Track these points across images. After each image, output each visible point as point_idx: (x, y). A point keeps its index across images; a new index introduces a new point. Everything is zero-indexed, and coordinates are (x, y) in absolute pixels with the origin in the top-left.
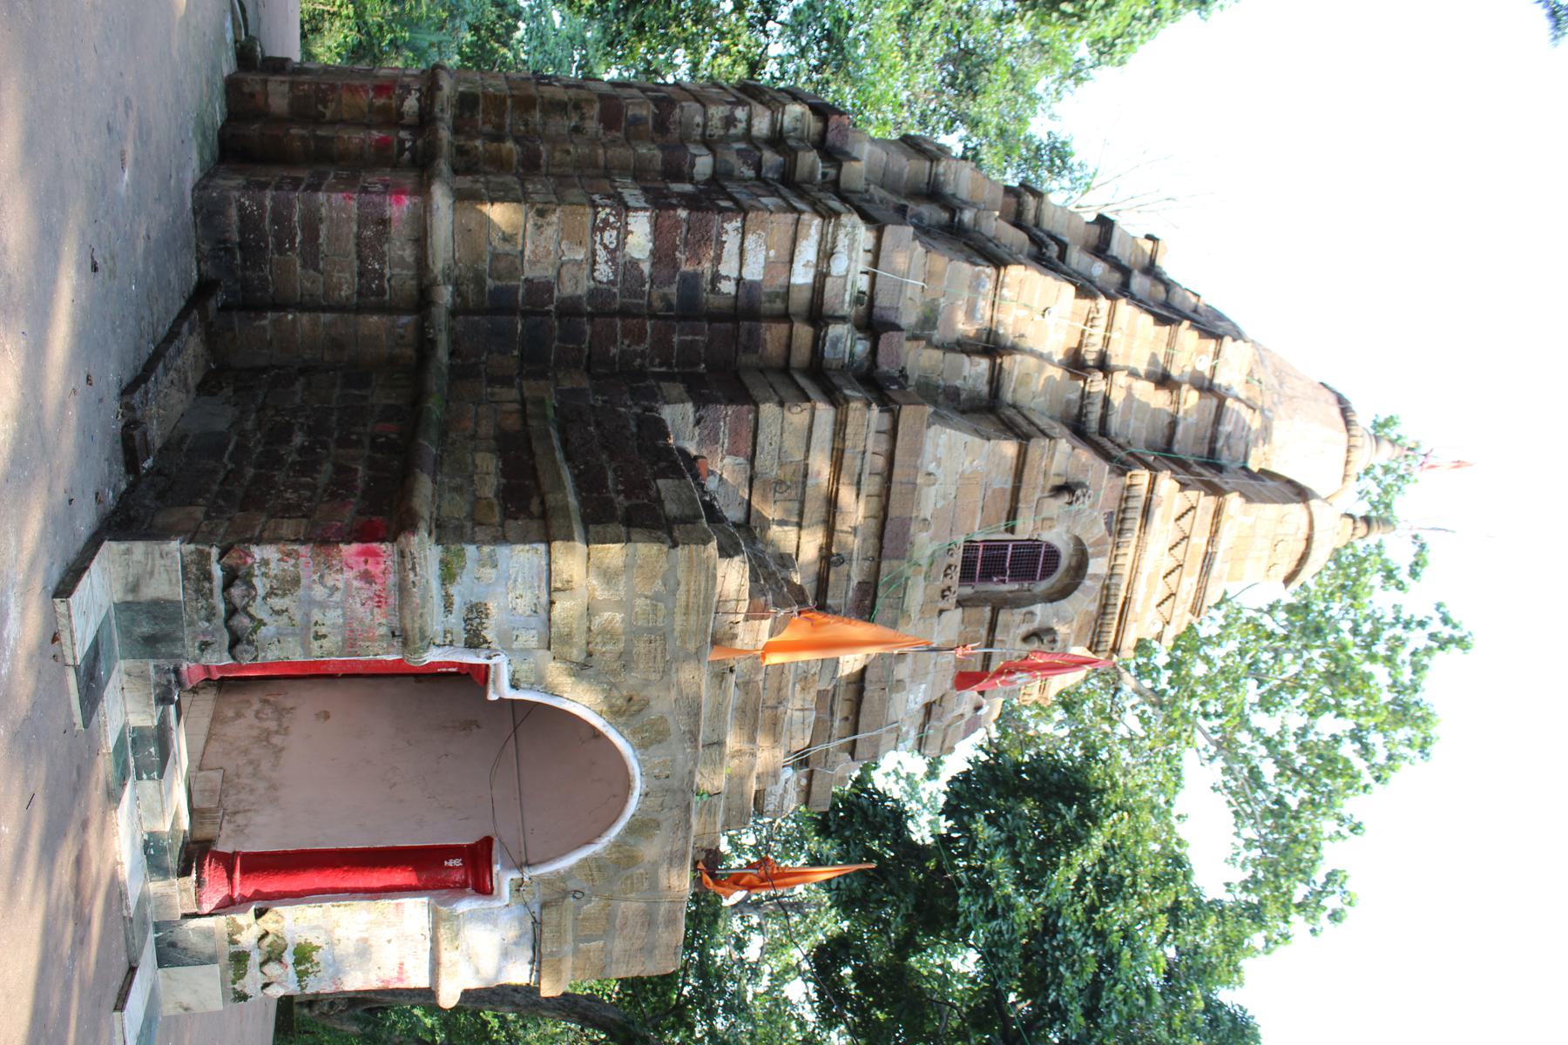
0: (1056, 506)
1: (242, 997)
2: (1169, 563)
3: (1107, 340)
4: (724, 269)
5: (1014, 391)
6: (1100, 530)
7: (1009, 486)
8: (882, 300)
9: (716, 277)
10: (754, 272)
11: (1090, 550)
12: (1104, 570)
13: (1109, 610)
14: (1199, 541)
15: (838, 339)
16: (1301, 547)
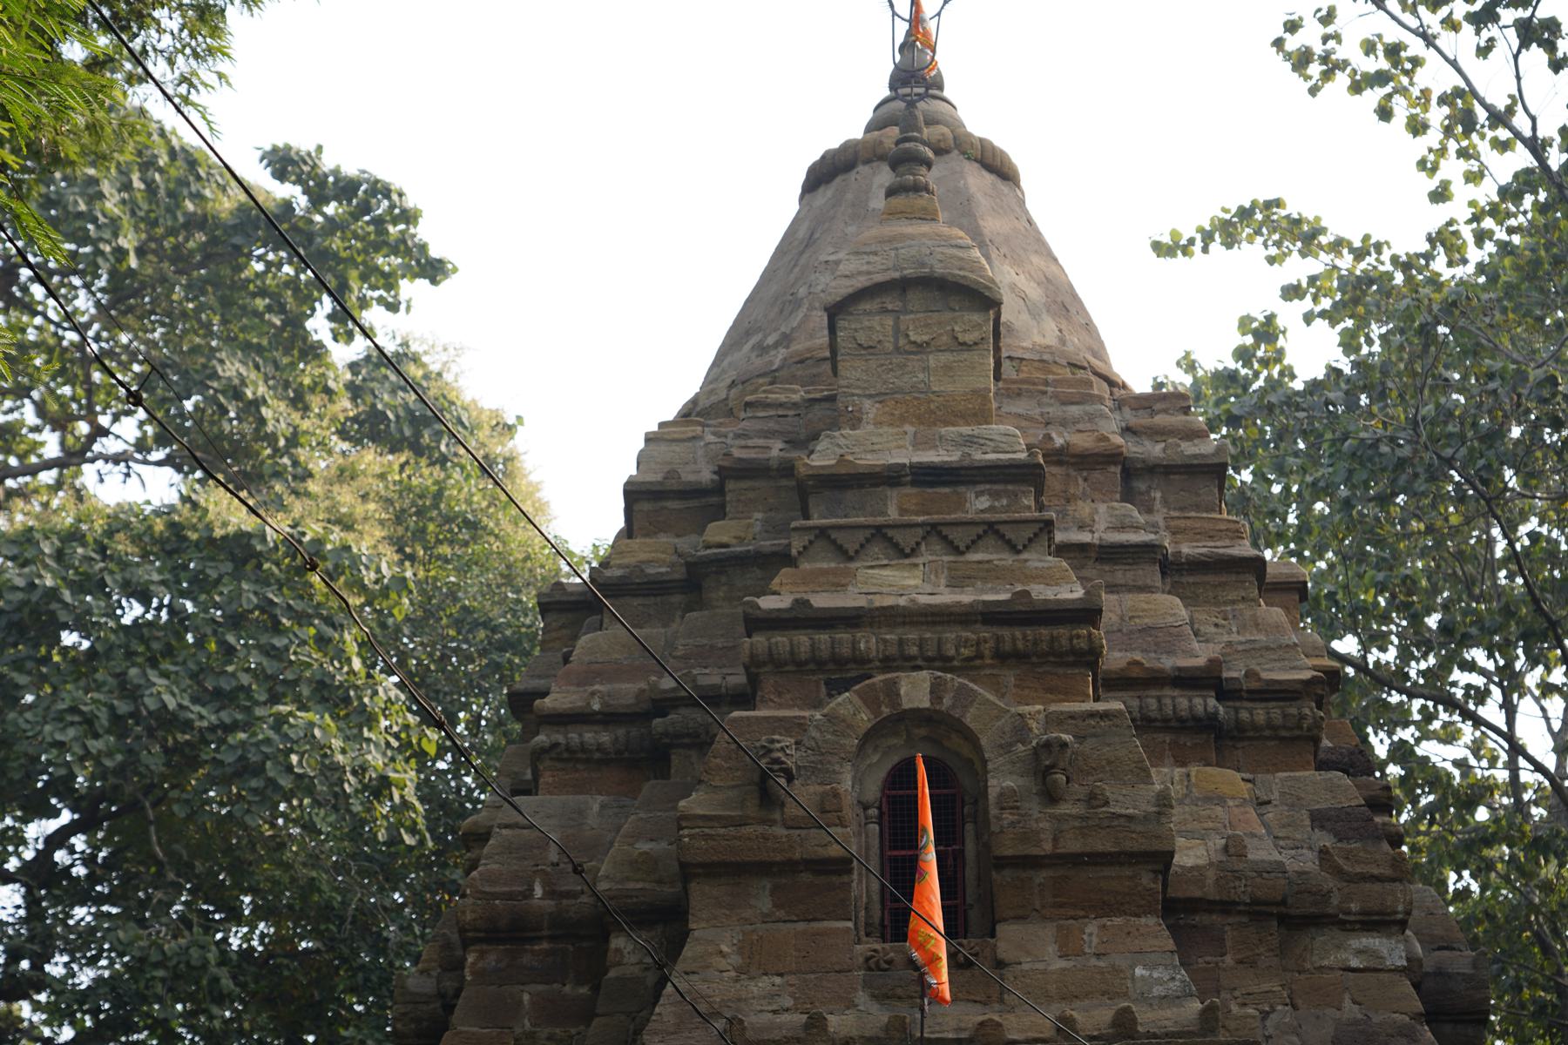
2: (932, 555)
3: (608, 718)
5: (660, 882)
6: (845, 702)
7: (768, 884)
11: (886, 711)
12: (924, 677)
13: (1008, 647)
14: (894, 507)
16: (915, 298)
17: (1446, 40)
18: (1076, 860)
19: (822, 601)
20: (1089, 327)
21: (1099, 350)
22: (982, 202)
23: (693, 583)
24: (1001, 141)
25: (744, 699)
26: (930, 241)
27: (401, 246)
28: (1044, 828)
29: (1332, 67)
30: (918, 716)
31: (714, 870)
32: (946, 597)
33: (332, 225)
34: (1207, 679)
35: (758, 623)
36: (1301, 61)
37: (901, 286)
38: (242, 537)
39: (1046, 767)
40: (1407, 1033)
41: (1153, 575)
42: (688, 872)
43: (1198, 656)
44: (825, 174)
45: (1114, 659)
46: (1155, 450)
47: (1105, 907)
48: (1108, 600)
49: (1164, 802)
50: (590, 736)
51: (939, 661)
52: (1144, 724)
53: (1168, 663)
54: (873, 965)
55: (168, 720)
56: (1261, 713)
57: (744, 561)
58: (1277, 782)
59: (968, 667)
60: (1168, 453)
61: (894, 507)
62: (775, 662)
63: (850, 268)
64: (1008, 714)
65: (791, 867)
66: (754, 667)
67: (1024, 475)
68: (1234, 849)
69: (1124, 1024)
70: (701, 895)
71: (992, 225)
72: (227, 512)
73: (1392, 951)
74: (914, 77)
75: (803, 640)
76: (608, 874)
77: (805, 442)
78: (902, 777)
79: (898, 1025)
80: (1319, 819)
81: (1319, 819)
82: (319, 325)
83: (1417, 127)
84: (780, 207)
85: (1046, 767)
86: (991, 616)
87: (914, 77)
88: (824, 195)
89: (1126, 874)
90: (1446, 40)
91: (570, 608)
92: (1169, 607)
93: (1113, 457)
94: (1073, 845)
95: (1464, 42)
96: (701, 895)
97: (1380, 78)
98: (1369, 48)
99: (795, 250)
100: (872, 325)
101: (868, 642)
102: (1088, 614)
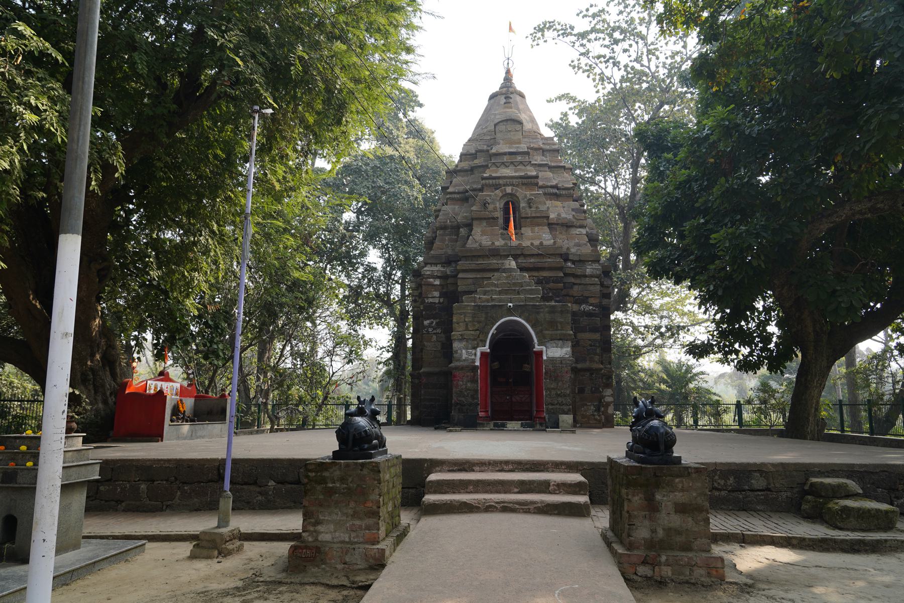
0: (490, 207)
1: (569, 410)
2: (512, 167)
3: (459, 193)
4: (437, 301)
8: (443, 260)
9: (439, 303)
10: (437, 294)
12: (510, 188)
14: (505, 159)
15: (451, 272)
17: (600, 65)
18: (534, 217)
19: (494, 175)
20: (537, 124)
21: (538, 129)
22: (519, 103)
23: (472, 170)
24: (522, 91)
25: (481, 190)
26: (511, 112)
27: (415, 101)
28: (529, 212)
29: (579, 68)
30: (509, 194)
31: (477, 219)
32: (514, 174)
33: (403, 98)
34: (556, 187)
35: (483, 178)
36: (574, 67)
37: (507, 120)
38: (391, 156)
39: (530, 203)
40: (586, 245)
41: (547, 169)
42: (473, 219)
43: (554, 183)
44: (493, 97)
45: (541, 183)
46: (548, 147)
47: (539, 225)
48: (540, 174)
49: (548, 208)
50: (456, 196)
51: (513, 185)
52: (545, 194)
53: (549, 184)
54: (502, 234)
55: (380, 187)
56: (564, 192)
57: (480, 167)
58: (566, 204)
59: (517, 186)
60: (548, 149)
61: (505, 159)
62: (486, 185)
63: (499, 118)
64: (523, 194)
65: (489, 218)
66: (483, 186)
67: (527, 153)
68: (559, 215)
69: (541, 243)
70: (475, 223)
71: (521, 107)
72: (389, 151)
73: (584, 231)
74: (508, 78)
75: (491, 181)
76: (459, 219)
77: (491, 146)
78: (507, 204)
79: (506, 244)
80: (573, 210)
81: (573, 210)
82: (401, 115)
83: (594, 80)
84: (485, 103)
85: (530, 203)
86: (521, 177)
87: (508, 78)
88: (492, 101)
89: (543, 220)
90: (600, 65)
91: (453, 173)
92: (549, 174)
93: (541, 149)
94: (534, 215)
95: (603, 66)
96: (475, 223)
97: (588, 71)
98: (586, 65)
99: (487, 111)
100: (502, 127)
101: (501, 182)
102: (537, 177)
